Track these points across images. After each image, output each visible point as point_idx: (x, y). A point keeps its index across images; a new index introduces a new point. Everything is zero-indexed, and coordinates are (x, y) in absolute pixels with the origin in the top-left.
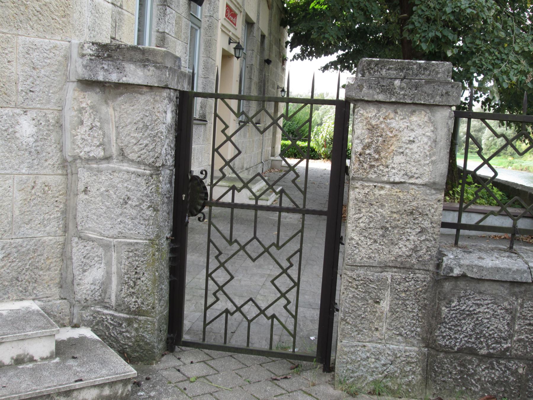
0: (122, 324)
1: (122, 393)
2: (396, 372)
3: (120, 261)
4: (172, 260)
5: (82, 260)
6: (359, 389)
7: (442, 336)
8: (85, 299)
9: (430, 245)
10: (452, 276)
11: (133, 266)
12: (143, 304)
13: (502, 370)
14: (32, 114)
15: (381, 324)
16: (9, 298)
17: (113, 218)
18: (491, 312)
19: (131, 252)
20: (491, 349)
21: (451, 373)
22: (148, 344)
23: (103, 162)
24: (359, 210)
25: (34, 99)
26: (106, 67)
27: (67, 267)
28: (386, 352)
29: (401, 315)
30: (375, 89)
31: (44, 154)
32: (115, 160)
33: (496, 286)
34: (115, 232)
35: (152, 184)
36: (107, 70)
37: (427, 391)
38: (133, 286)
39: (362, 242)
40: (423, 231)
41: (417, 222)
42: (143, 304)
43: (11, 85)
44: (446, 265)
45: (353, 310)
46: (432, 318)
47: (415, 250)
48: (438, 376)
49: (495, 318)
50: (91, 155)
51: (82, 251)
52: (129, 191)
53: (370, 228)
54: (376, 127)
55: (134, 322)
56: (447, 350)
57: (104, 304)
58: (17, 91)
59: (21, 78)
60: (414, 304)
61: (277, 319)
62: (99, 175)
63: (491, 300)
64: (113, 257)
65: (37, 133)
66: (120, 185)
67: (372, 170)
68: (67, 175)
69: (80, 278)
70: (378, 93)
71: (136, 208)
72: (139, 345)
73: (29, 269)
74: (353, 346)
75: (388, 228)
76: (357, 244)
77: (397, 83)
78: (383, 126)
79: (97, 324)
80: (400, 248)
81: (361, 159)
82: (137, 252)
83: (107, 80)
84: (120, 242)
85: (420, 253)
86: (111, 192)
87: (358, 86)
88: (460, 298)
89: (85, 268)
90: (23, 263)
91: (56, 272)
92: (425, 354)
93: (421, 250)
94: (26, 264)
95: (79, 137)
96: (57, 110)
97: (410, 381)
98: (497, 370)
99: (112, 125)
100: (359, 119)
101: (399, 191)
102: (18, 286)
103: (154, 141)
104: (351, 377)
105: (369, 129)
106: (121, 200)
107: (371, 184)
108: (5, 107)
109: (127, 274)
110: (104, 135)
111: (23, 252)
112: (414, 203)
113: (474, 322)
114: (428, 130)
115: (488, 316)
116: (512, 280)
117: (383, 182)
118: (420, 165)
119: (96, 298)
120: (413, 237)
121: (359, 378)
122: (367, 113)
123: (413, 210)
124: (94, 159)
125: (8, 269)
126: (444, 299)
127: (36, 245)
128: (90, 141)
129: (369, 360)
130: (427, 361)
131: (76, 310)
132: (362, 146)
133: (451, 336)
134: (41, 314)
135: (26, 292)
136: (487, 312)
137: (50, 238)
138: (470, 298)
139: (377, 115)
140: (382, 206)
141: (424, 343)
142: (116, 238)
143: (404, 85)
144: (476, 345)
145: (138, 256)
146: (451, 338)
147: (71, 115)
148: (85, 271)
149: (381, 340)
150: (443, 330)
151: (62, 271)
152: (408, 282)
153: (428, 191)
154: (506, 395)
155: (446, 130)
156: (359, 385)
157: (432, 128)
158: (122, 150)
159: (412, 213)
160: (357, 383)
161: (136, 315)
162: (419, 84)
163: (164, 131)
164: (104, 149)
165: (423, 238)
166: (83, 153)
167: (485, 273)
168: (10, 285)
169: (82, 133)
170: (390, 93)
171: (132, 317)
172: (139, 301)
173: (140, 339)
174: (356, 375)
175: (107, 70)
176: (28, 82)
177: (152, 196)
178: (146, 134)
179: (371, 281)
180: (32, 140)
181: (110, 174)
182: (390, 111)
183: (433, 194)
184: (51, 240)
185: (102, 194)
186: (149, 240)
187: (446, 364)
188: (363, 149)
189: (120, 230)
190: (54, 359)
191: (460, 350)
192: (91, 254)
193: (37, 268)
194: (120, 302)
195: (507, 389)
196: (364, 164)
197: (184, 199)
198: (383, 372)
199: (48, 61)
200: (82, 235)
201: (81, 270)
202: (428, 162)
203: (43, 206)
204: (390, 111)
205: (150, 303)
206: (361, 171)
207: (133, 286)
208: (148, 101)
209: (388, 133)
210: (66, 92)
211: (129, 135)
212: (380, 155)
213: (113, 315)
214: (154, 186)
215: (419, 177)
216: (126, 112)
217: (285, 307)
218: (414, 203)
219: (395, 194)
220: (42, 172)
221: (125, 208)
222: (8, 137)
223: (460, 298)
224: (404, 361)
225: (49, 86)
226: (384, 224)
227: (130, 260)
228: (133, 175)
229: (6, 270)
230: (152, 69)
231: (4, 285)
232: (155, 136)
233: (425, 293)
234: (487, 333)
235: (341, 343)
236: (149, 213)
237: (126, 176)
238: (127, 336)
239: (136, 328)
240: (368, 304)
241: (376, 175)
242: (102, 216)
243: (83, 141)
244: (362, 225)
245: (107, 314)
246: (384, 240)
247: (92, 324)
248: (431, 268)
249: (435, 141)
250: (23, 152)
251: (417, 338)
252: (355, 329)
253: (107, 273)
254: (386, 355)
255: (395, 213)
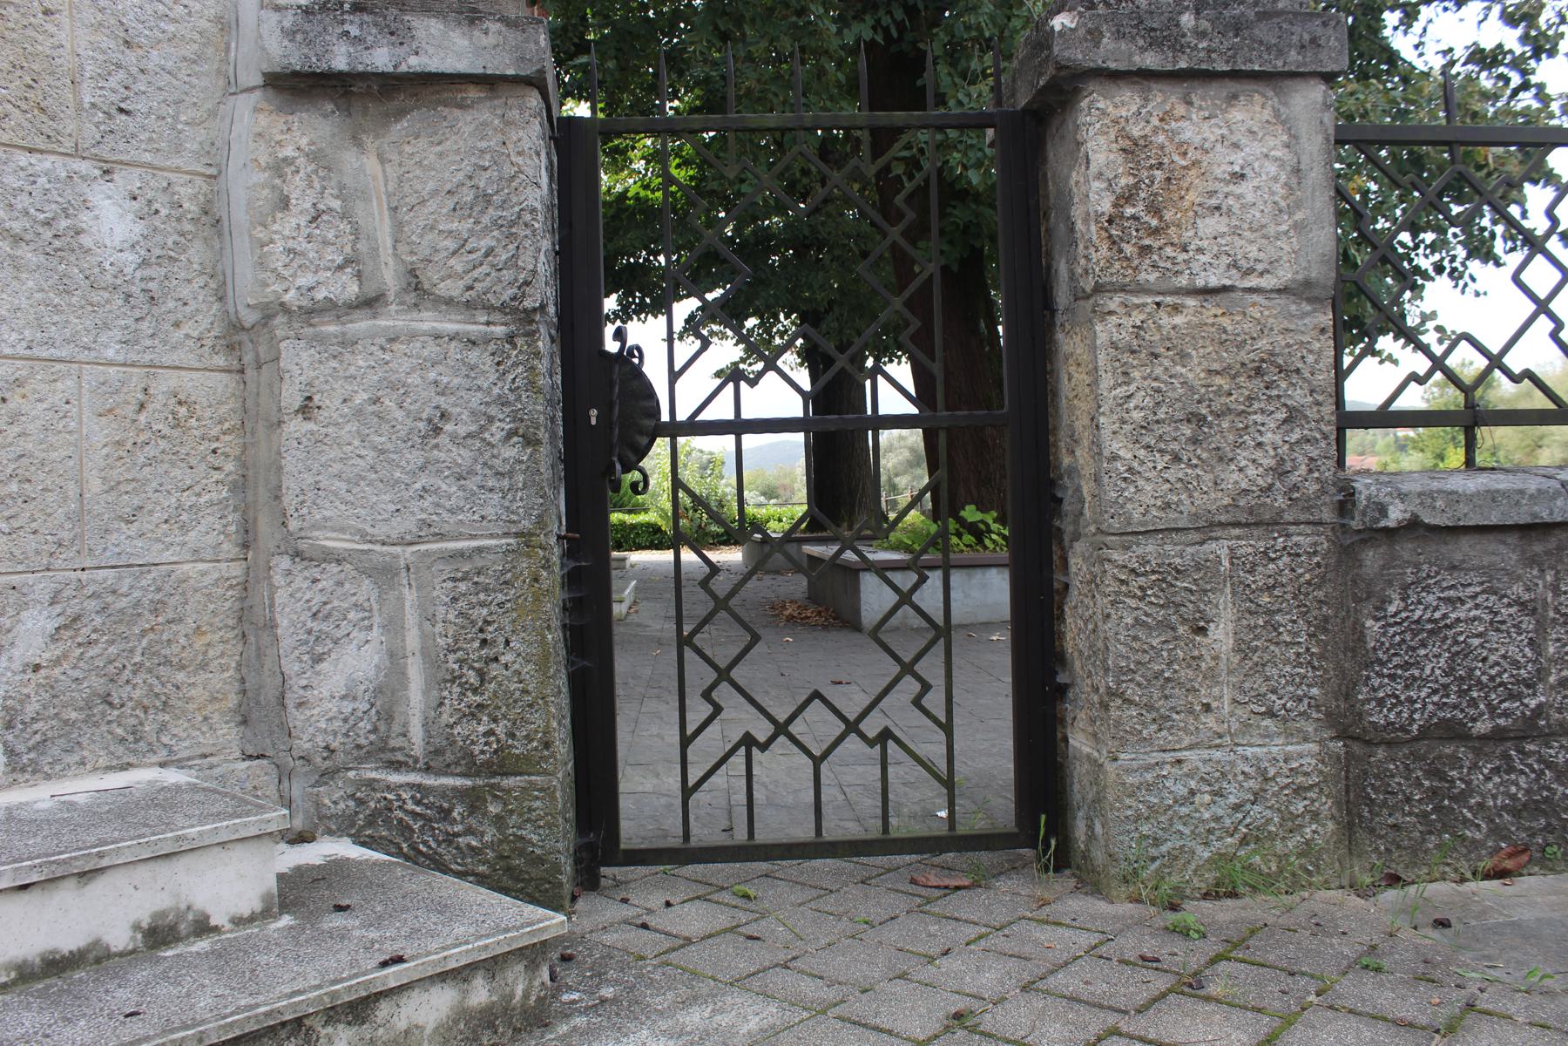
0: (450, 811)
1: (526, 996)
2: (1269, 821)
3: (431, 611)
4: (573, 608)
5: (310, 624)
6: (1175, 888)
7: (1375, 699)
8: (327, 748)
9: (1314, 454)
10: (1386, 530)
11: (473, 623)
12: (512, 735)
13: (1533, 771)
14: (128, 180)
15: (1216, 690)
16: (83, 763)
17: (397, 482)
18: (1487, 617)
19: (462, 579)
20: (1500, 716)
21: (1408, 800)
22: (540, 860)
23: (357, 314)
24: (1126, 374)
25: (133, 136)
26: (354, 31)
27: (260, 655)
28: (1238, 771)
29: (1267, 657)
30: (1133, 38)
31: (171, 304)
32: (393, 307)
33: (1490, 544)
34: (405, 525)
35: (516, 365)
36: (358, 40)
37: (1355, 861)
38: (477, 684)
39: (1142, 463)
40: (1293, 416)
41: (1274, 392)
42: (512, 735)
43: (58, 84)
44: (1369, 498)
45: (1139, 663)
46: (1346, 656)
47: (1280, 471)
48: (1377, 815)
49: (1498, 630)
50: (320, 295)
51: (307, 597)
52: (442, 394)
53: (1158, 422)
54: (1142, 142)
55: (489, 798)
56: (1391, 737)
57: (388, 756)
58: (79, 108)
59: (90, 69)
60: (1294, 622)
61: (898, 742)
62: (348, 356)
63: (1482, 583)
64: (408, 605)
65: (145, 238)
66: (414, 379)
67: (1147, 261)
68: (242, 371)
69: (304, 682)
70: (1143, 50)
71: (469, 441)
72: (508, 870)
73: (141, 665)
74: (1148, 768)
75: (1205, 418)
76: (1130, 470)
77: (1187, 20)
78: (1161, 138)
79: (370, 822)
80: (1241, 470)
81: (1114, 232)
82: (481, 579)
83: (361, 68)
84: (427, 554)
85: (1294, 478)
86: (387, 402)
87: (1089, 32)
88: (1405, 588)
89: (319, 649)
90: (123, 646)
91: (226, 675)
92: (1339, 758)
93: (1295, 468)
94: (131, 651)
95: (279, 247)
96: (203, 175)
97: (1307, 843)
98: (1522, 772)
99: (380, 205)
100: (1098, 126)
101: (1220, 312)
102: (109, 722)
103: (511, 236)
104: (1154, 859)
105: (1124, 150)
106: (421, 425)
107: (1149, 300)
108: (41, 152)
109: (455, 652)
110: (356, 232)
111: (121, 611)
112: (1263, 343)
113: (1448, 650)
114: (1275, 144)
115: (1481, 629)
116: (1529, 520)
117: (1178, 292)
118: (1265, 237)
119: (362, 741)
120: (1269, 435)
121: (1173, 857)
122: (1116, 107)
123: (1263, 361)
124: (331, 308)
125: (75, 667)
126: (1368, 598)
127: (159, 590)
128: (311, 255)
129: (1197, 799)
130: (1347, 778)
131: (297, 789)
132: (1113, 199)
133: (1397, 697)
134: (204, 789)
135: (137, 741)
136: (1475, 619)
137: (201, 566)
138: (1428, 586)
139: (1144, 111)
140: (1183, 356)
141: (1331, 727)
142: (411, 544)
143: (1205, 25)
144: (1462, 711)
145: (486, 590)
146: (1400, 703)
147: (251, 183)
148: (318, 659)
149: (1220, 736)
150: (1376, 682)
151: (244, 670)
152: (1273, 560)
153: (1293, 307)
154: (1551, 838)
155: (1320, 138)
156: (1175, 879)
157: (1285, 138)
158: (412, 272)
159: (1259, 372)
160: (1170, 874)
161: (494, 774)
162: (1243, 20)
163: (538, 205)
164: (359, 275)
165: (1295, 437)
166: (292, 293)
167: (1463, 508)
168: (85, 721)
169: (287, 233)
170: (1172, 47)
171: (480, 782)
172: (500, 730)
173: (513, 850)
174: (1164, 849)
175: (358, 40)
176: (113, 82)
177: (519, 399)
178: (485, 220)
179: (1178, 571)
180: (131, 258)
181: (382, 348)
182: (1173, 99)
183: (1307, 314)
184: (204, 574)
185: (359, 412)
186: (517, 535)
187: (1393, 776)
188: (1115, 206)
189: (424, 516)
190: (276, 918)
191: (1424, 733)
192: (336, 603)
193: (167, 662)
194: (439, 741)
195: (1554, 822)
196: (1124, 245)
197: (593, 422)
198: (1236, 829)
199: (171, 28)
200: (303, 545)
201: (306, 657)
202: (1284, 227)
203: (173, 464)
204: (1173, 99)
205: (536, 731)
206: (1117, 265)
207: (477, 684)
208: (484, 124)
209: (1176, 158)
210: (228, 121)
211: (432, 228)
212: (1161, 219)
213: (419, 785)
214: (520, 369)
215: (1268, 272)
216: (419, 163)
217: (917, 702)
218: (1263, 343)
219: (1211, 320)
220: (167, 359)
221: (436, 446)
222: (57, 243)
223: (1405, 588)
224: (1287, 786)
225: (178, 102)
226: (1193, 408)
227: (462, 604)
228: (453, 344)
229: (70, 672)
230: (494, 27)
231: (66, 722)
232: (512, 224)
233: (1319, 587)
234: (1483, 673)
235: (1115, 765)
236: (510, 452)
237: (432, 349)
238: (469, 845)
239: (497, 816)
240: (1176, 638)
241: (1157, 274)
242: (363, 478)
243: (290, 259)
244: (1137, 415)
245: (401, 786)
246: (1199, 451)
247: (353, 825)
248: (1327, 515)
249: (1297, 171)
250: (106, 295)
251: (1315, 715)
252: (1149, 717)
253: (391, 655)
254: (1241, 778)
255: (1218, 373)
